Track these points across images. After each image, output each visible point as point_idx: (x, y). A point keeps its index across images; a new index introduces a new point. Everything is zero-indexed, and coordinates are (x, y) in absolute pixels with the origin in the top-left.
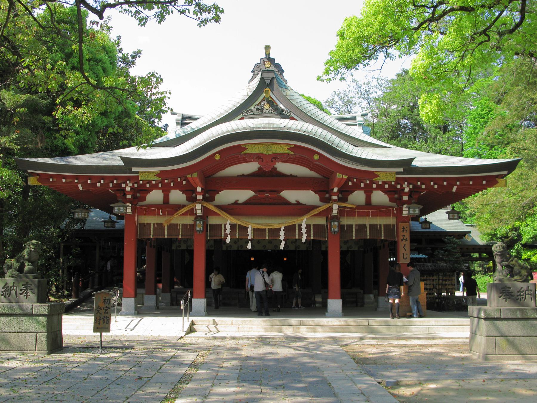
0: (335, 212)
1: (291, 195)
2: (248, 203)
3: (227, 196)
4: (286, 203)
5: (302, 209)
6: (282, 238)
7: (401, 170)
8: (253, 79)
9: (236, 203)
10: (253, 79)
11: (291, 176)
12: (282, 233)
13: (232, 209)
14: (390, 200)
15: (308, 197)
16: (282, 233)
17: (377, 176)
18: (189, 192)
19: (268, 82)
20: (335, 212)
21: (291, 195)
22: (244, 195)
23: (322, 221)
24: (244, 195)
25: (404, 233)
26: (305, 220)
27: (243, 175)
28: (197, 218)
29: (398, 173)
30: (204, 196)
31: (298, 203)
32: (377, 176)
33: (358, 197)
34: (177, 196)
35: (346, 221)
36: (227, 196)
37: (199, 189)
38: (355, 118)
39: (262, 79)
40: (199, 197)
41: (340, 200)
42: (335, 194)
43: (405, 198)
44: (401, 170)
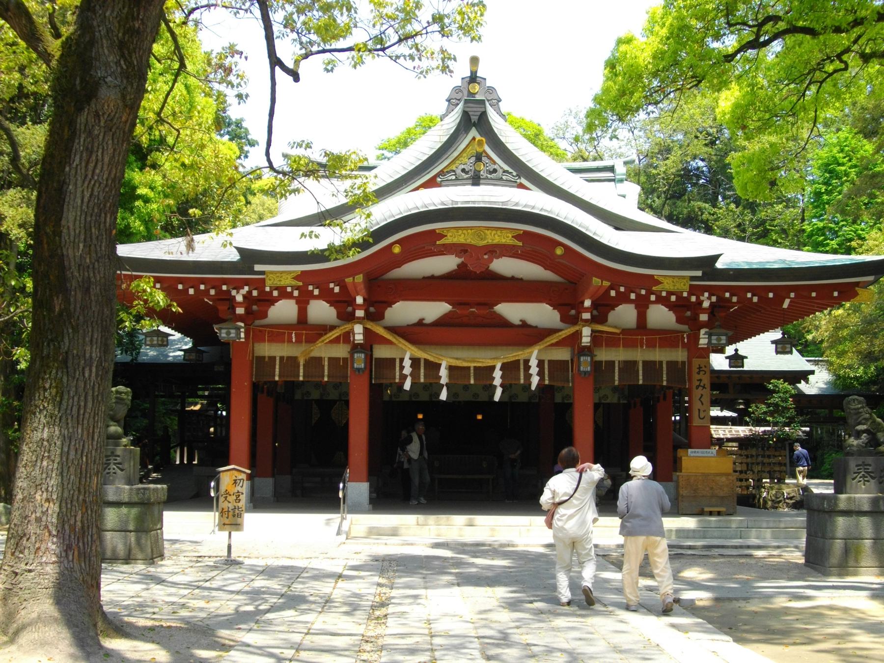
0: (586, 340)
1: (512, 311)
2: (442, 322)
3: (406, 311)
4: (504, 324)
5: (530, 335)
6: (497, 381)
7: (699, 273)
9: (420, 323)
10: (448, 112)
11: (513, 278)
12: (498, 374)
13: (414, 333)
14: (679, 320)
15: (540, 314)
16: (498, 374)
17: (658, 283)
18: (343, 304)
19: (474, 119)
20: (586, 340)
21: (512, 311)
22: (433, 310)
23: (563, 354)
24: (433, 310)
25: (701, 376)
26: (535, 353)
27: (432, 277)
28: (356, 348)
29: (693, 278)
30: (366, 311)
31: (524, 325)
32: (658, 283)
33: (625, 315)
34: (321, 311)
35: (603, 355)
36: (406, 311)
37: (359, 300)
38: (611, 169)
39: (466, 115)
40: (360, 313)
41: (594, 320)
42: (586, 310)
43: (704, 317)
44: (699, 273)
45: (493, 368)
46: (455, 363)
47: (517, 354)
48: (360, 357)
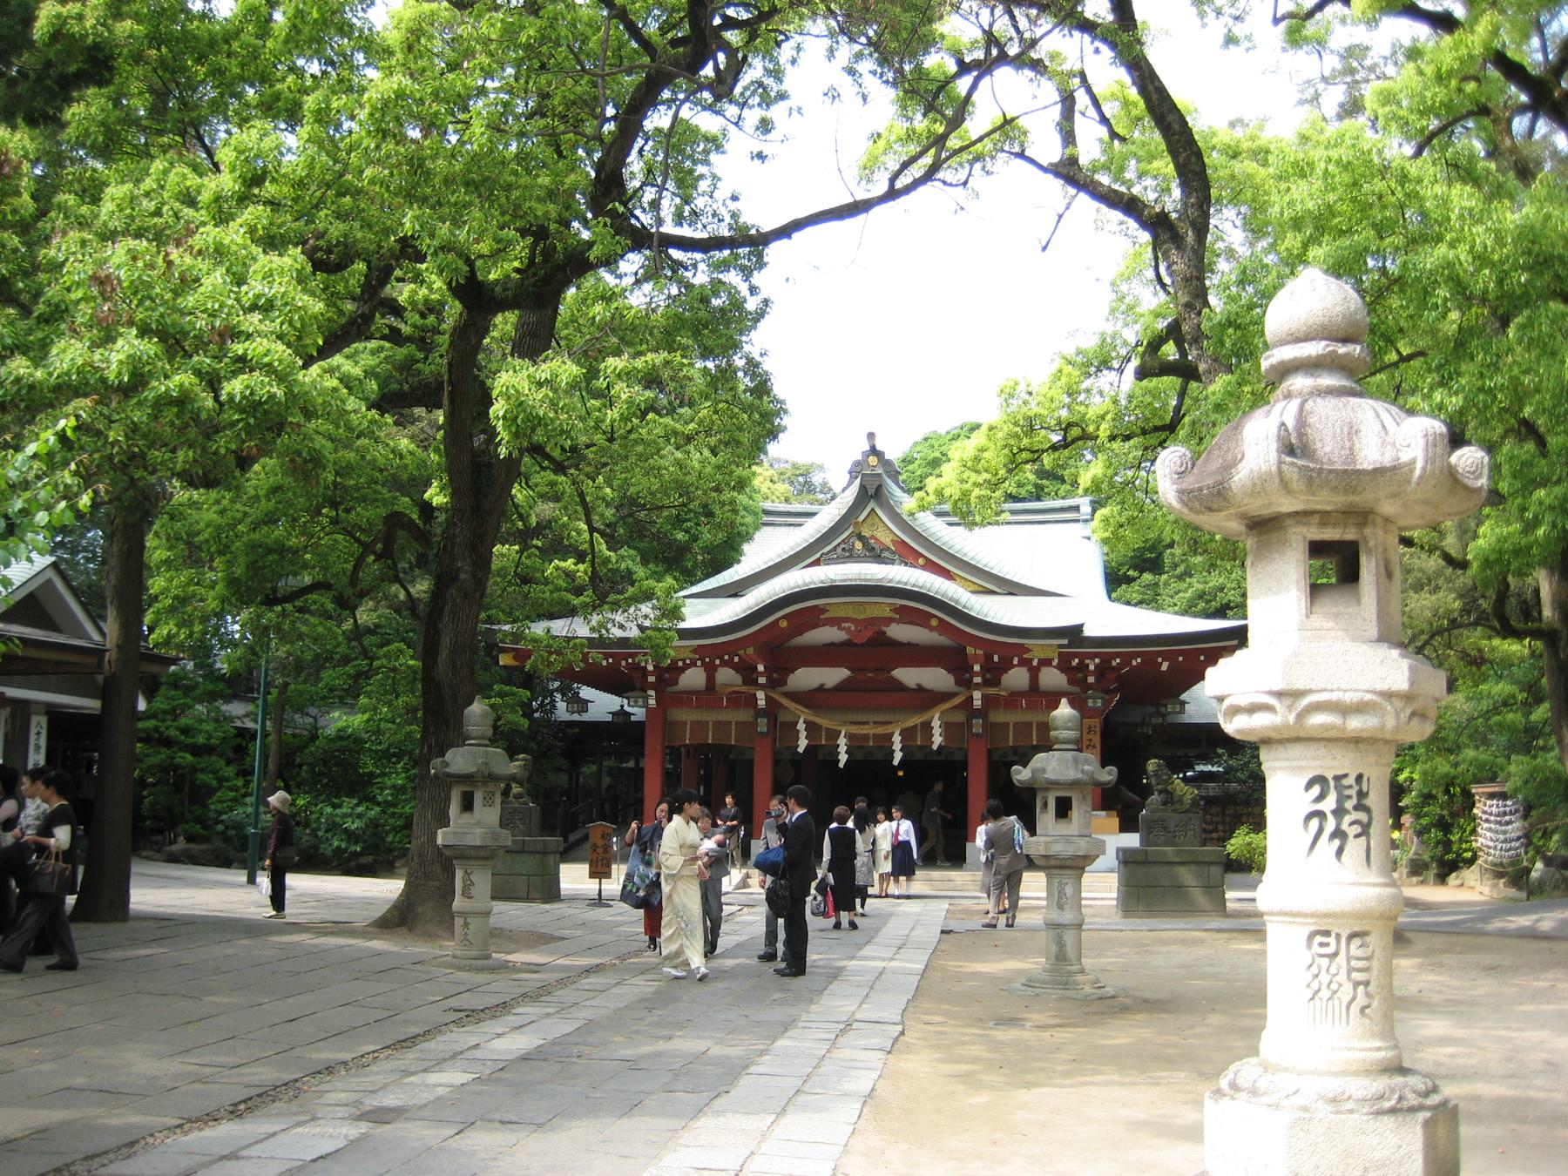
0: (977, 703)
1: (909, 676)
2: (842, 687)
3: (806, 678)
4: (899, 687)
5: (926, 699)
6: (897, 746)
7: (1066, 642)
8: (849, 485)
9: (821, 688)
10: (849, 485)
11: (909, 644)
12: (897, 739)
13: (814, 699)
14: (1070, 682)
15: (935, 678)
16: (897, 739)
17: (1028, 650)
18: (747, 671)
19: (871, 491)
20: (977, 703)
21: (909, 676)
22: (833, 676)
23: (960, 717)
24: (833, 676)
25: (1091, 736)
26: (937, 716)
27: (832, 644)
28: (760, 713)
29: (1060, 646)
30: (769, 679)
31: (920, 688)
32: (1028, 650)
33: (1017, 678)
34: (726, 676)
35: (998, 717)
36: (806, 678)
37: (761, 668)
38: (1077, 508)
39: (863, 487)
40: (762, 680)
41: (986, 683)
42: (977, 674)
43: (1091, 679)
44: (1066, 642)
45: (892, 735)
46: (855, 729)
47: (915, 720)
48: (763, 725)
